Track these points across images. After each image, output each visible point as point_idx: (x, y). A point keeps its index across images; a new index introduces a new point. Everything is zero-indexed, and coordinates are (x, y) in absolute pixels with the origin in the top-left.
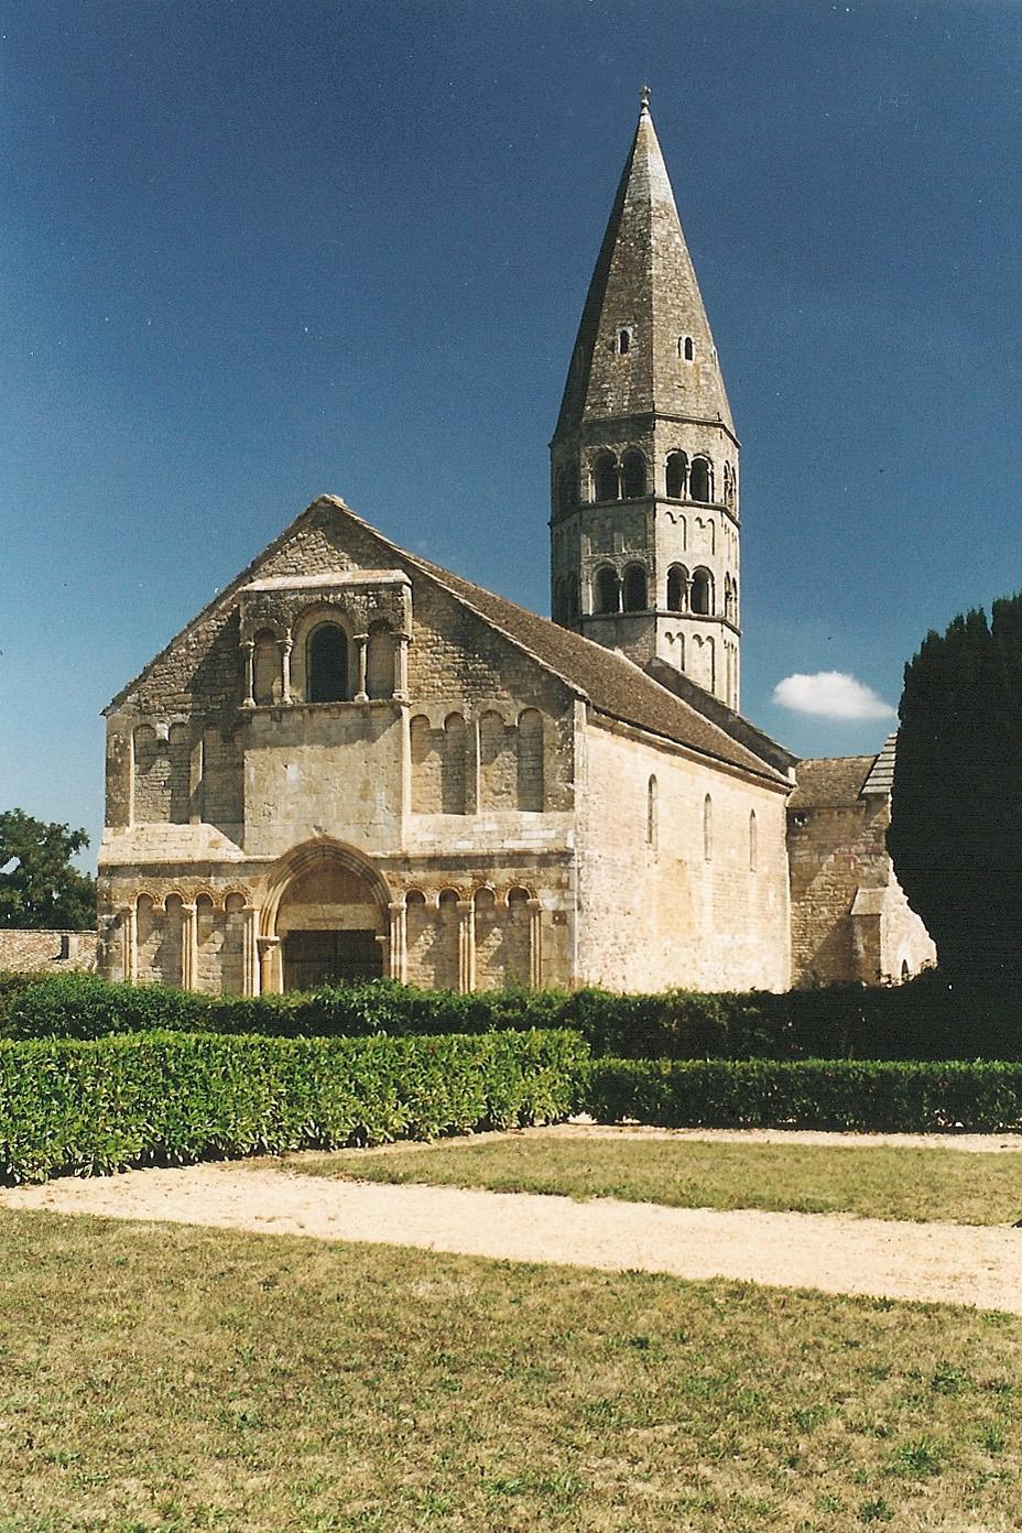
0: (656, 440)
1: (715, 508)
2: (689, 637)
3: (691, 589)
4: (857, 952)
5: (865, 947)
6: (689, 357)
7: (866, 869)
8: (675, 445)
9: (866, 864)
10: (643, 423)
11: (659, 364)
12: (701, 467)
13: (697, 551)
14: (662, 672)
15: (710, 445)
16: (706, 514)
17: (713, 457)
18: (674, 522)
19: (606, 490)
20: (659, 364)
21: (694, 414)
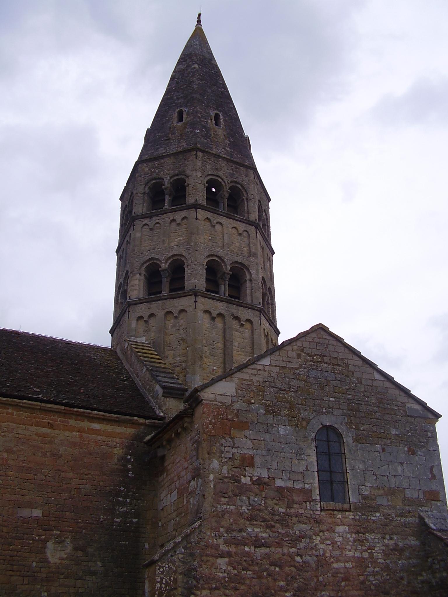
6: (180, 119)
13: (172, 244)
16: (179, 216)
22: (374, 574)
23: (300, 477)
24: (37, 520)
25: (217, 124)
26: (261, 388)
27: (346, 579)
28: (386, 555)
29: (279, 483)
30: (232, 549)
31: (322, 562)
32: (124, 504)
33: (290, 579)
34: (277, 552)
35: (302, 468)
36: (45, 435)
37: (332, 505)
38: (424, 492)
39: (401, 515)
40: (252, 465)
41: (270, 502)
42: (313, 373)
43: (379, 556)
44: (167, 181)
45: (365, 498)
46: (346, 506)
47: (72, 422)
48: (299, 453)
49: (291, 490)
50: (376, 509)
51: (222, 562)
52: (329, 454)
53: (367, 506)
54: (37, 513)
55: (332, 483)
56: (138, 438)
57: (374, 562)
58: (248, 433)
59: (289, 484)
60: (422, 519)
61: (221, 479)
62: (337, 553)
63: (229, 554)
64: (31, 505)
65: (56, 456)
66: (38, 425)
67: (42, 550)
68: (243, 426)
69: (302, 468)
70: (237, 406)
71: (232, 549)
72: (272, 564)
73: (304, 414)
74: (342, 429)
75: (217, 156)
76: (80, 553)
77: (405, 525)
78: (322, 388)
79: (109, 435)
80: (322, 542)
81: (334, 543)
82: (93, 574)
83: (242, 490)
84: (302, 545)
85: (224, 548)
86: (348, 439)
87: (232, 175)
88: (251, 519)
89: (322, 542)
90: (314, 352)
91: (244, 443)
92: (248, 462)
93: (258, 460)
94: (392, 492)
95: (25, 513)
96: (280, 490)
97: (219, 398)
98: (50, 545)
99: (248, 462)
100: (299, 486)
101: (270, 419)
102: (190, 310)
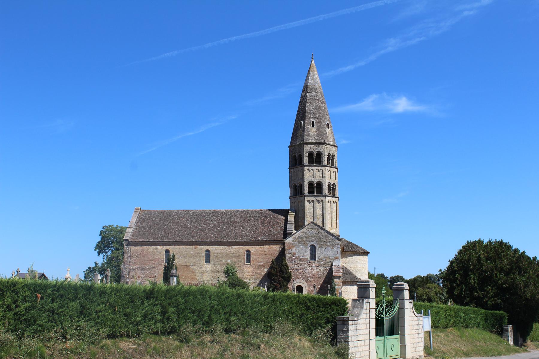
25: (313, 126)
26: (298, 238)
31: (309, 273)
48: (306, 251)
53: (320, 261)
54: (262, 264)
55: (313, 257)
57: (321, 272)
61: (289, 258)
68: (294, 247)
75: (311, 144)
86: (317, 247)
91: (294, 250)
94: (326, 258)
95: (260, 264)
96: (301, 259)
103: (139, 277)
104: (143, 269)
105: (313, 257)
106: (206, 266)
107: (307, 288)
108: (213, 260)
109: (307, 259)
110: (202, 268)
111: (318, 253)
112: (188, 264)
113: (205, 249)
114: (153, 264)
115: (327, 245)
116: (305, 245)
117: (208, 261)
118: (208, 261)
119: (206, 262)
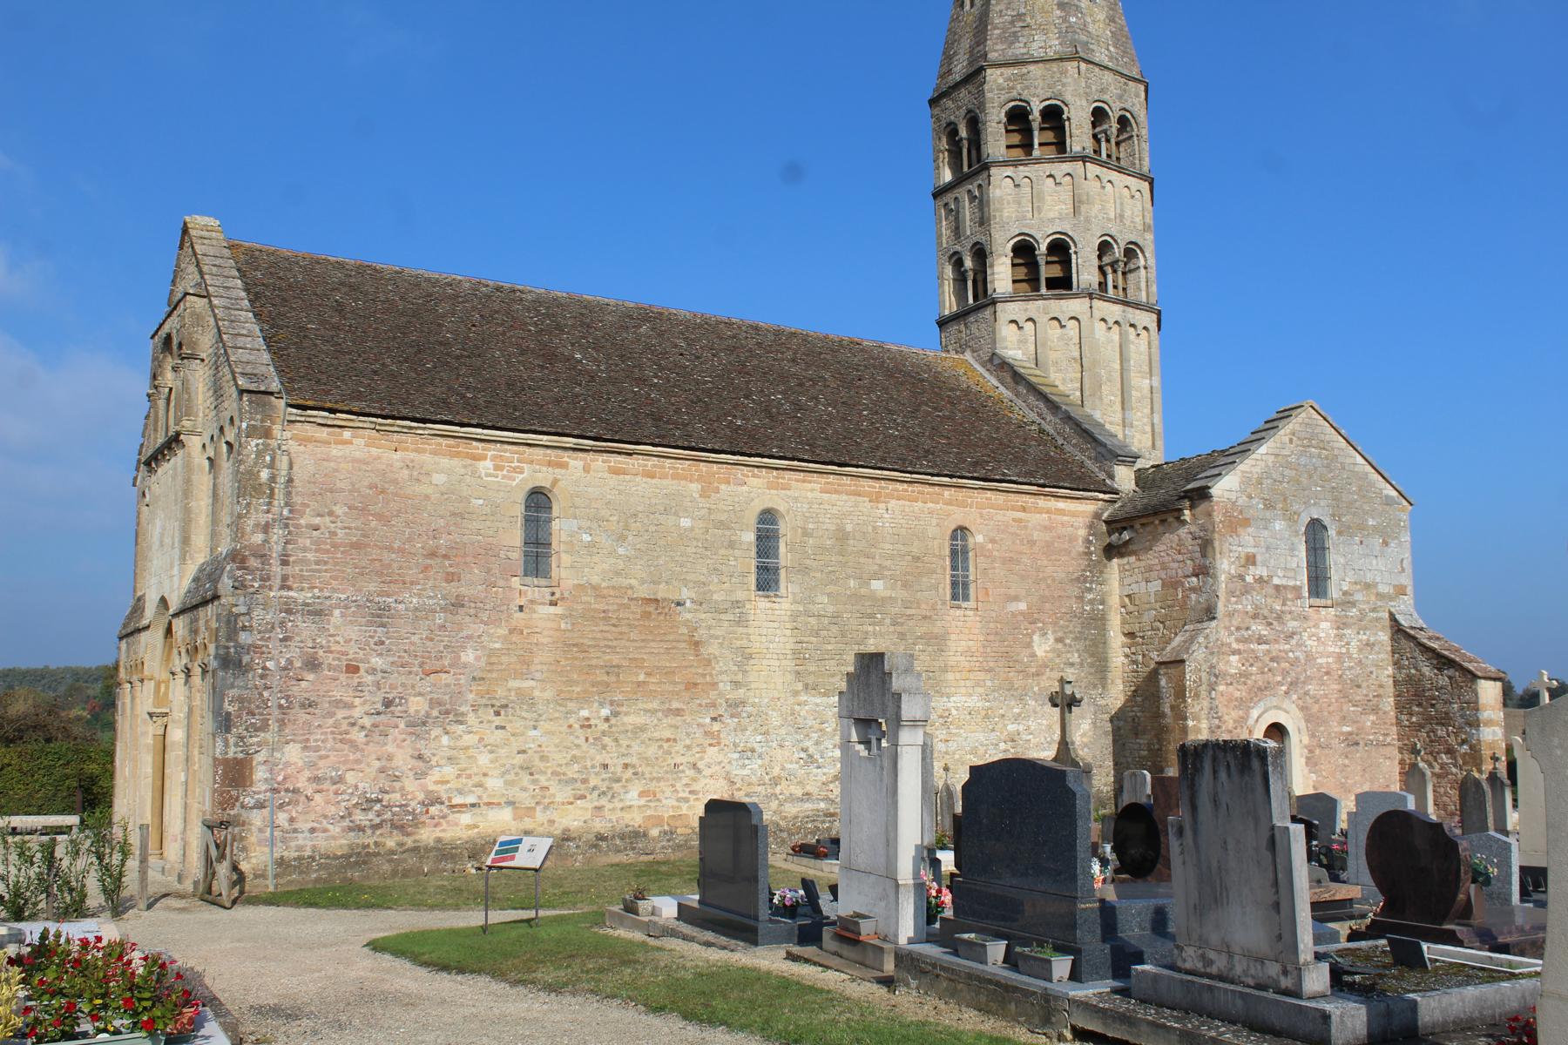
0: (988, 95)
1: (1074, 159)
2: (1042, 320)
3: (1047, 268)
4: (1164, 715)
5: (1172, 707)
7: (1193, 596)
8: (1014, 94)
9: (1193, 589)
10: (975, 76)
11: (998, 8)
12: (1054, 116)
13: (1051, 215)
14: (1003, 367)
15: (1064, 85)
16: (1061, 169)
17: (1068, 98)
18: (1017, 186)
19: (956, 164)
20: (998, 8)
21: (1037, 53)
22: (1350, 668)
23: (1291, 574)
24: (1022, 613)
27: (1327, 673)
28: (1360, 650)
29: (1276, 581)
30: (1241, 646)
31: (1310, 657)
32: (1090, 590)
33: (1285, 673)
34: (1275, 648)
35: (1294, 565)
36: (1020, 521)
37: (1317, 602)
38: (1395, 586)
39: (1374, 610)
40: (1254, 564)
41: (1269, 600)
42: (1303, 460)
43: (1354, 651)
44: (1036, 107)
45: (1345, 593)
46: (1329, 602)
47: (1042, 502)
48: (1292, 549)
49: (1285, 587)
50: (1353, 604)
51: (1234, 659)
52: (1315, 549)
53: (1347, 602)
54: (1022, 606)
56: (1097, 516)
57: (1350, 658)
58: (1250, 530)
59: (1284, 582)
60: (1391, 614)
61: (1231, 578)
62: (1321, 649)
63: (1237, 652)
64: (1016, 598)
65: (1032, 543)
66: (1013, 509)
67: (1029, 645)
68: (1246, 522)
69: (1294, 565)
70: (1240, 502)
71: (1241, 646)
72: (1272, 660)
73: (1295, 507)
74: (1327, 521)
76: (1060, 646)
77: (1377, 619)
78: (1311, 477)
79: (1074, 514)
80: (1310, 638)
81: (1319, 639)
82: (1072, 665)
83: (1247, 590)
84: (1293, 642)
85: (1235, 646)
86: (1332, 532)
87: (1120, 97)
88: (1255, 616)
89: (1310, 638)
90: (1303, 435)
91: (1247, 541)
92: (1251, 560)
93: (1259, 558)
94: (1368, 586)
96: (1277, 587)
97: (1227, 495)
98: (1036, 637)
99: (1251, 560)
100: (1291, 583)
101: (1268, 514)
102: (1084, 318)
103: (353, 669)
104: (380, 615)
105: (1318, 582)
106: (761, 605)
107: (1306, 740)
108: (805, 570)
109: (1297, 589)
110: (741, 621)
111: (1335, 560)
112: (662, 592)
113: (758, 506)
114: (451, 578)
115: (1362, 527)
116: (1291, 518)
117: (767, 580)
118: (767, 580)
119: (760, 587)
